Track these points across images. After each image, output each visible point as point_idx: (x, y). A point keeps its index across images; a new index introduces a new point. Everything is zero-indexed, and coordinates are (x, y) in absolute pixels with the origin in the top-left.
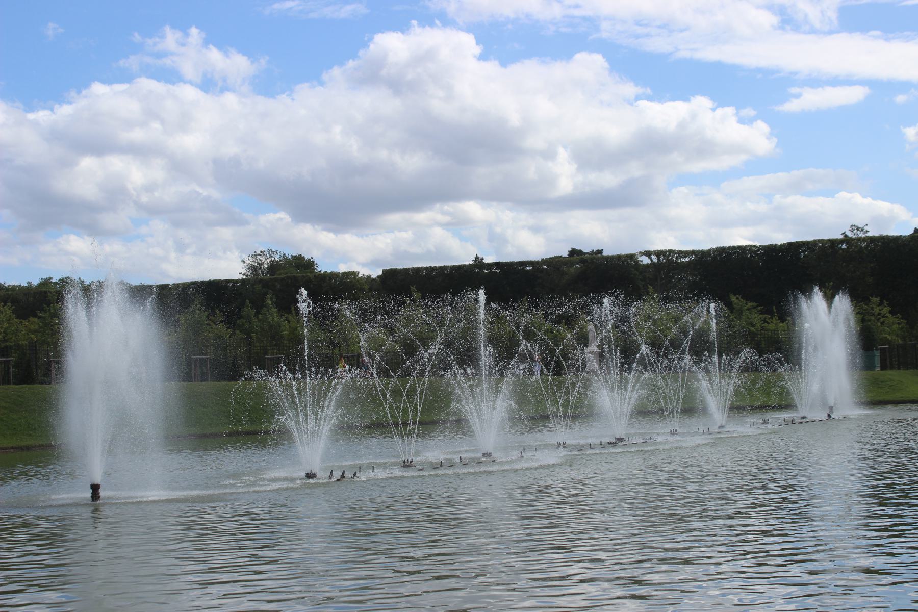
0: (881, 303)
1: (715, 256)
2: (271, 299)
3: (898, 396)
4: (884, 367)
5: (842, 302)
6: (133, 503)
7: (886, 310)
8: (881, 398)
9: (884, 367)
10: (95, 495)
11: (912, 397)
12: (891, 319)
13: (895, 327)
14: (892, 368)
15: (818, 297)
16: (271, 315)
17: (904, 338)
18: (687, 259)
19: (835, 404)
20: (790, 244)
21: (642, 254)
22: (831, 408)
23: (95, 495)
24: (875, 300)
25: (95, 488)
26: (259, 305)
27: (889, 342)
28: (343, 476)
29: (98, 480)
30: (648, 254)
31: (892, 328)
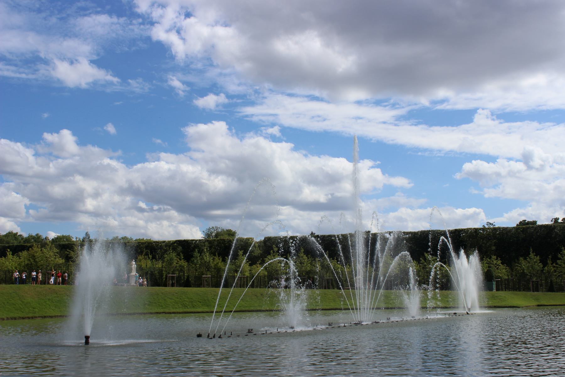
0: (497, 259)
1: (420, 235)
2: (207, 249)
3: (503, 304)
4: (498, 290)
5: (475, 258)
7: (499, 262)
8: (495, 305)
9: (498, 290)
10: (87, 342)
11: (510, 305)
12: (502, 266)
13: (504, 271)
14: (502, 290)
16: (206, 256)
17: (508, 276)
19: (471, 307)
20: (456, 230)
21: (387, 233)
22: (469, 309)
23: (87, 342)
24: (495, 257)
25: (87, 338)
26: (201, 252)
27: (500, 277)
28: (214, 337)
29: (88, 334)
31: (502, 271)
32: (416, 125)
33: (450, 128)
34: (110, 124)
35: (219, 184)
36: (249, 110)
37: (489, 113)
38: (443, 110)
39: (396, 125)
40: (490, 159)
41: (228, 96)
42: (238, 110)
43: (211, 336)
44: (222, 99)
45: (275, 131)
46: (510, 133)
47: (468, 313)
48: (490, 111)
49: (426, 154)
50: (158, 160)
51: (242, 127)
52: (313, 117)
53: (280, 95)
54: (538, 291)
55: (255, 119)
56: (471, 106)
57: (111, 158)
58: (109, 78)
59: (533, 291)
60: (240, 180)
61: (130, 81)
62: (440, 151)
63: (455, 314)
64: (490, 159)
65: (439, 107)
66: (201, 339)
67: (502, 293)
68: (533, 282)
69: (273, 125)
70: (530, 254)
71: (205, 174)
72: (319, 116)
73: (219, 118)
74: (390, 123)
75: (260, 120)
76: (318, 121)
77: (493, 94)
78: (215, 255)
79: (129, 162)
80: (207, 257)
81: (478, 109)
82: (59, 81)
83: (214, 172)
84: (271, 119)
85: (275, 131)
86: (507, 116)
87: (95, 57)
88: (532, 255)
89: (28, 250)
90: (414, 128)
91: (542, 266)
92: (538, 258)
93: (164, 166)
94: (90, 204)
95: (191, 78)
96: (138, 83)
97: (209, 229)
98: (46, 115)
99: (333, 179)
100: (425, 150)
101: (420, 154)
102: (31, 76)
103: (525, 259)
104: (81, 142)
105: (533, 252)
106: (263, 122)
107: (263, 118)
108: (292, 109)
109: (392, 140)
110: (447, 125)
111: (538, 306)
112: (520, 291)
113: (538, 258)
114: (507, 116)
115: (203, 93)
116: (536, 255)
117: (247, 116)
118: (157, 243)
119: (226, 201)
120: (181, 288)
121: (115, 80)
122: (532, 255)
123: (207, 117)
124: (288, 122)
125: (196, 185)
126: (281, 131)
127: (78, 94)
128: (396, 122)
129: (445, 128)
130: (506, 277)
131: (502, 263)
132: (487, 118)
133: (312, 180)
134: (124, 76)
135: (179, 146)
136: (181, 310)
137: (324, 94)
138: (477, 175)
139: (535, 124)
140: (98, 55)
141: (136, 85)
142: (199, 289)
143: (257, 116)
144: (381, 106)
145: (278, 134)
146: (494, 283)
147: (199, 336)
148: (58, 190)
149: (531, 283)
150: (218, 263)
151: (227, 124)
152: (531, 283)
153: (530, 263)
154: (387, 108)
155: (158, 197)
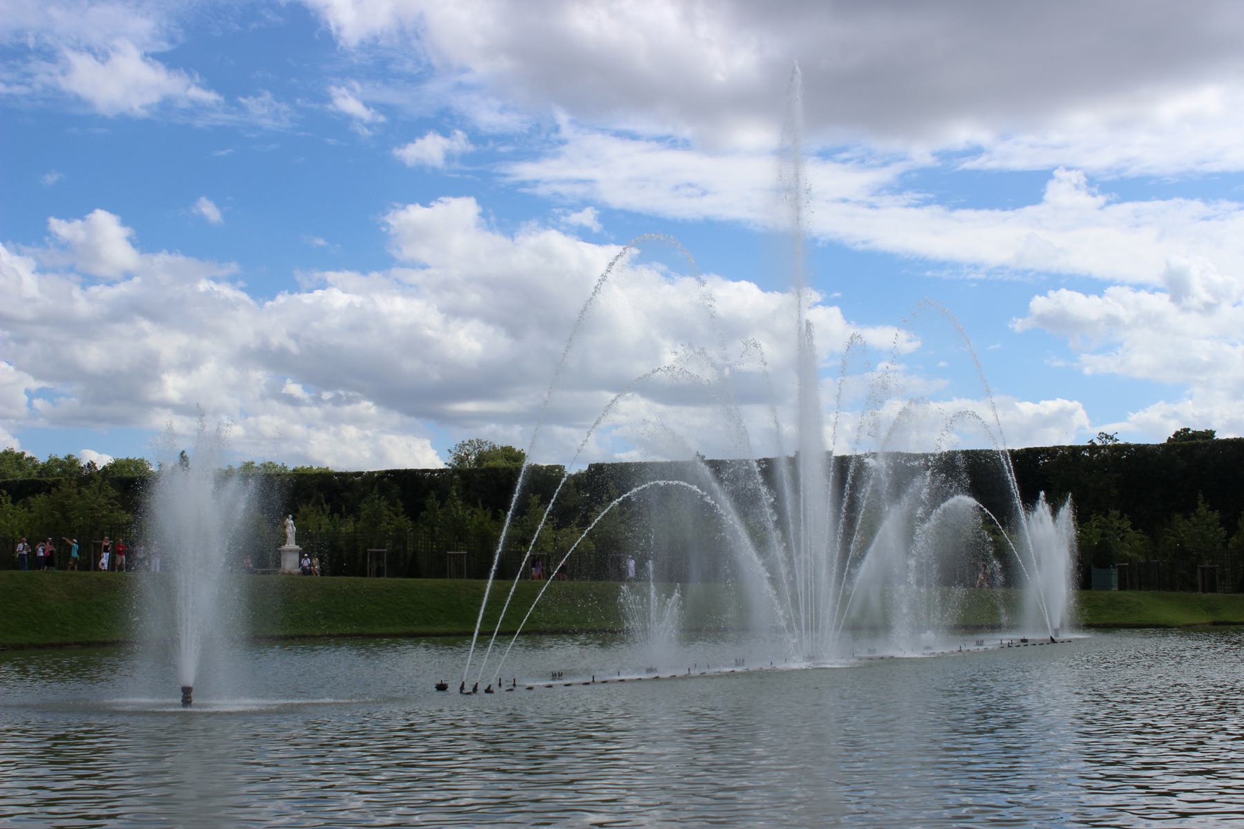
0: (1122, 517)
2: (457, 490)
3: (1133, 619)
6: (209, 715)
7: (1127, 524)
8: (1117, 621)
9: (1120, 589)
12: (1132, 533)
13: (1137, 543)
14: (1132, 587)
15: (1043, 508)
16: (456, 507)
18: (916, 463)
20: (1028, 450)
21: (866, 456)
24: (1115, 512)
26: (443, 497)
30: (874, 455)
31: (1131, 544)
32: (917, 206)
33: (998, 213)
34: (203, 199)
35: (469, 343)
36: (527, 170)
37: (1083, 179)
38: (978, 171)
39: (872, 206)
40: (1092, 286)
41: (475, 136)
42: (503, 170)
43: (468, 688)
44: (459, 143)
45: (587, 217)
46: (1138, 226)
47: (1053, 641)
48: (1086, 176)
49: (945, 274)
50: (323, 285)
51: (511, 209)
52: (677, 187)
53: (599, 136)
54: (1214, 590)
55: (542, 191)
56: (1042, 161)
57: (216, 280)
58: (197, 93)
59: (1204, 591)
60: (514, 330)
61: (242, 100)
62: (976, 267)
63: (1024, 641)
64: (1092, 286)
65: (969, 164)
66: (441, 693)
67: (1131, 595)
68: (1203, 569)
69: (584, 204)
70: (1197, 506)
71: (435, 318)
72: (690, 185)
73: (457, 190)
74: (858, 203)
75: (555, 194)
76: (690, 196)
77: (1084, 133)
78: (476, 505)
79: (261, 290)
80: (459, 509)
81: (1056, 168)
82: (79, 100)
83: (454, 313)
84: (580, 190)
85: (587, 217)
86: (1122, 187)
87: (165, 47)
88: (1202, 509)
89: (49, 491)
90: (913, 212)
91: (1224, 534)
92: (1216, 515)
93: (338, 301)
94: (173, 386)
95: (389, 95)
96: (263, 105)
97: (463, 445)
98: (51, 179)
99: (727, 331)
100: (941, 265)
101: (929, 273)
102: (17, 90)
103: (1188, 517)
104: (144, 242)
105: (1204, 502)
106: (562, 196)
107: (563, 189)
108: (621, 167)
109: (864, 242)
110: (991, 208)
111: (1215, 624)
112: (1173, 589)
113: (1216, 515)
114: (1122, 187)
115: (415, 129)
116: (1212, 509)
117: (524, 184)
118: (344, 476)
119: (486, 382)
120: (397, 579)
121: (210, 97)
122: (1202, 509)
123: (428, 186)
124: (620, 197)
125: (415, 344)
126: (600, 219)
127: (124, 130)
128: (872, 199)
129: (985, 212)
130: (1142, 560)
131: (1134, 527)
132: (1077, 187)
133: (681, 331)
134: (232, 88)
135: (372, 254)
136: (399, 630)
137: (687, 132)
138: (1060, 323)
139: (1196, 206)
140: (172, 40)
141: (262, 110)
142: (439, 581)
143: (546, 183)
144: (835, 161)
145: (597, 228)
146: (1115, 572)
147: (442, 687)
148: (92, 356)
149: (1199, 571)
150: (482, 524)
151: (478, 202)
152: (1199, 571)
153: (1199, 526)
154: (849, 165)
155: (333, 373)
